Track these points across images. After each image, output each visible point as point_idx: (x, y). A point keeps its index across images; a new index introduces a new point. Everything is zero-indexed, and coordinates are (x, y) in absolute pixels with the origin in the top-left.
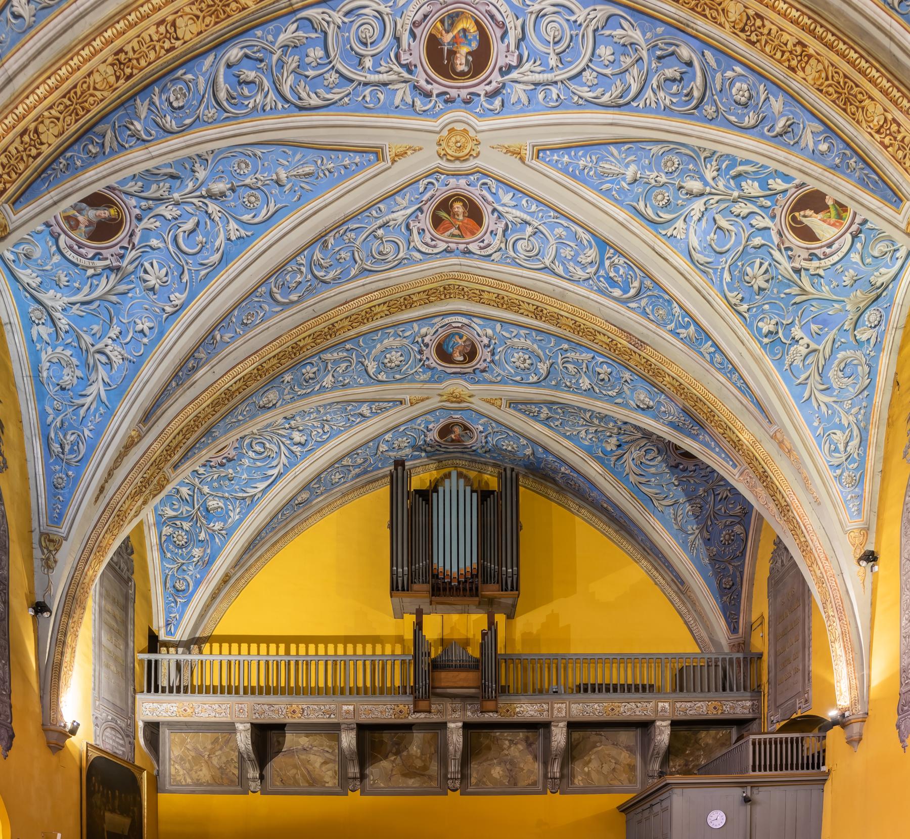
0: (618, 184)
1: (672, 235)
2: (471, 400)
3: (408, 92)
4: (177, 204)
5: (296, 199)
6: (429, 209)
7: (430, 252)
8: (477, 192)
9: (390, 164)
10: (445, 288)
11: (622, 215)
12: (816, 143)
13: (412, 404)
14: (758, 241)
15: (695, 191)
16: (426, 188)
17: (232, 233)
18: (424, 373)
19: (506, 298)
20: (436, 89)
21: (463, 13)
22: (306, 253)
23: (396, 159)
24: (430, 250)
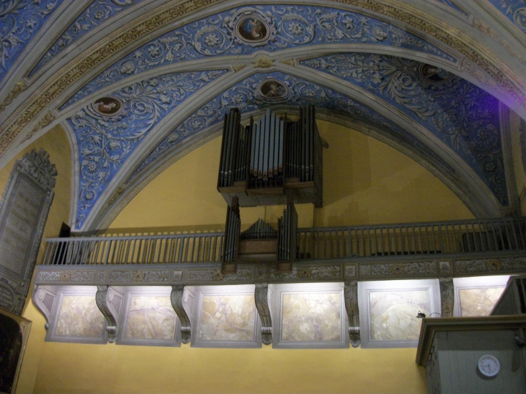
2: (274, 63)
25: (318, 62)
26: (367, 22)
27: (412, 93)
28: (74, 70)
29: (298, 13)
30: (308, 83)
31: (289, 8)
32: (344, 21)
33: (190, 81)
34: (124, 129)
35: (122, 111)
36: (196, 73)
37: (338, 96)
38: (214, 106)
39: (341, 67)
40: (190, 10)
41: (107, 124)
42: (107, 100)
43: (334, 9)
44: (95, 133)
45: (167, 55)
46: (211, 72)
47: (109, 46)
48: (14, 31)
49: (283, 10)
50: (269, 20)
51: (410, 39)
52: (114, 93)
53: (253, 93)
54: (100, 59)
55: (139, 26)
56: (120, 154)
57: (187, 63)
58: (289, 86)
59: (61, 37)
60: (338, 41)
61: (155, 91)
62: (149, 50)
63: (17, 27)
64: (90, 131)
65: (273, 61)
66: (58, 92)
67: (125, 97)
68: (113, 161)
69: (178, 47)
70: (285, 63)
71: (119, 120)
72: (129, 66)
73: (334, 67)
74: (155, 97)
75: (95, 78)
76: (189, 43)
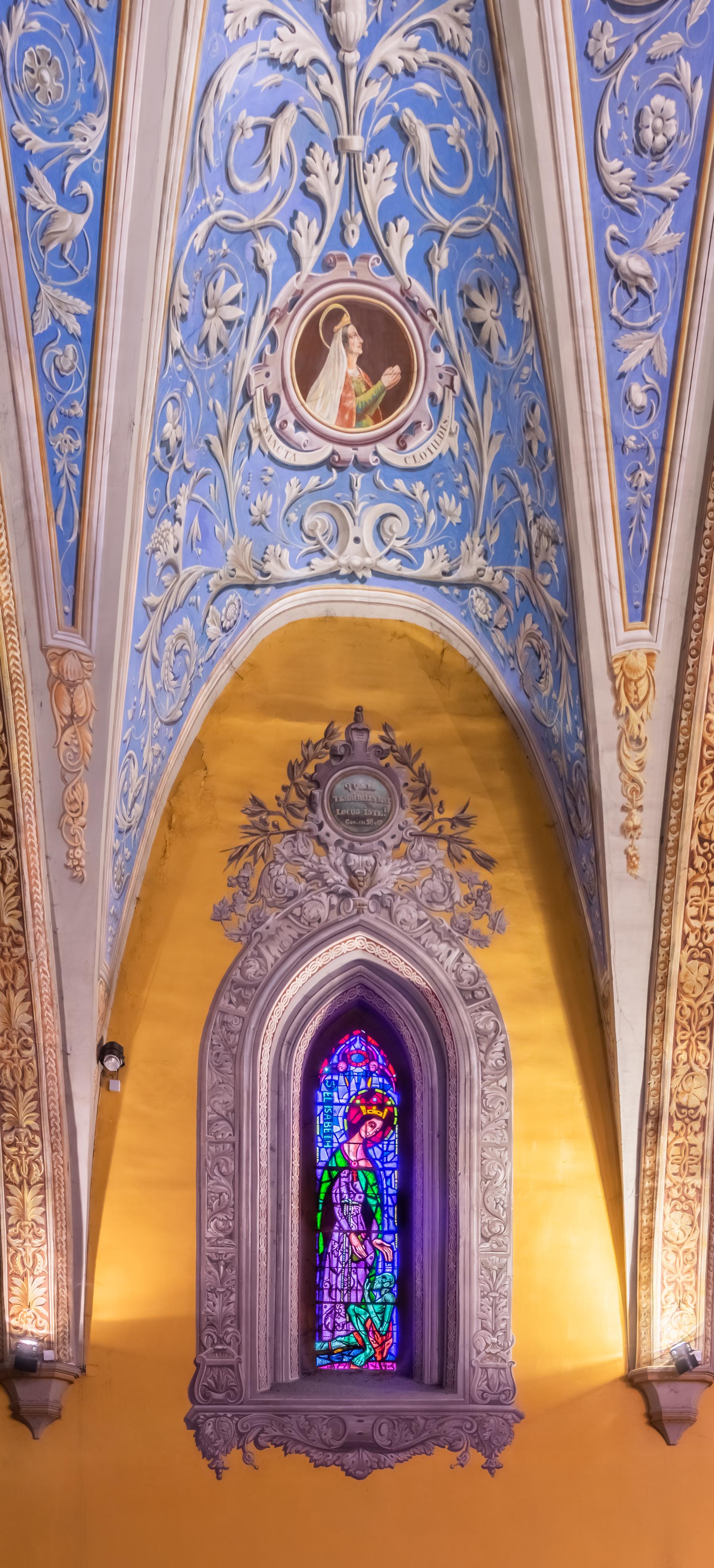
12: (637, 374)
15: (341, 16)
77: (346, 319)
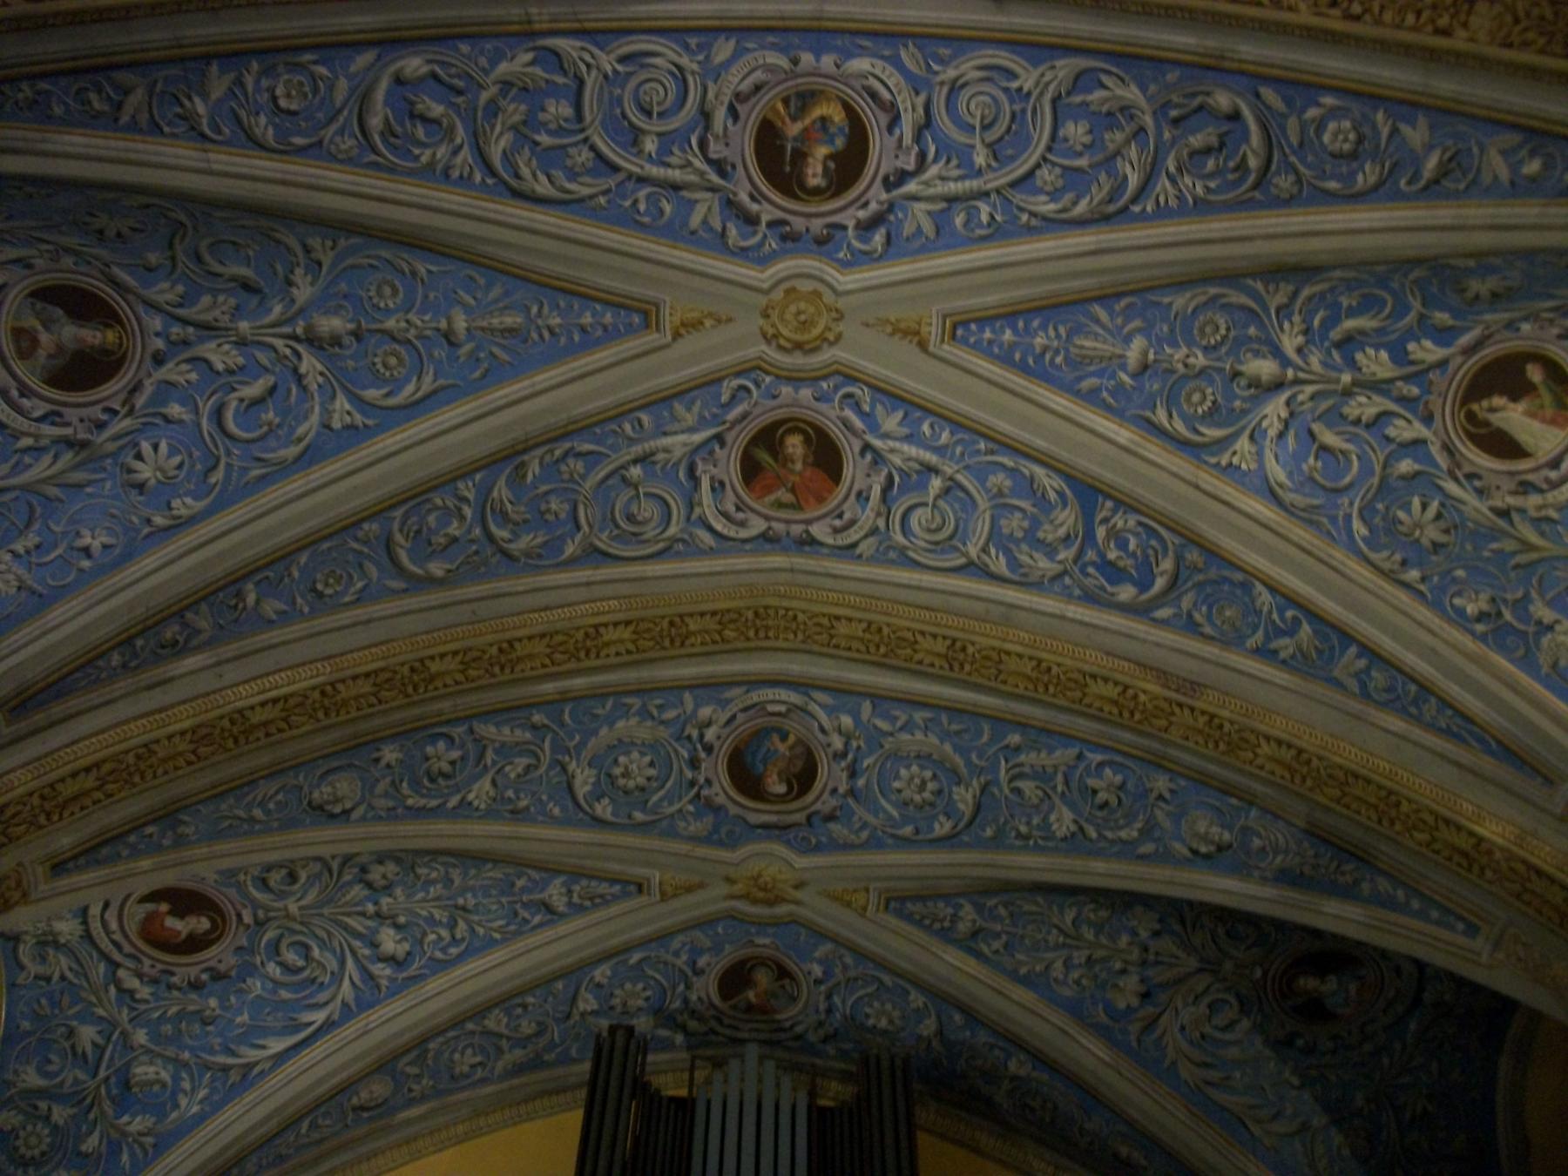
0: (1113, 376)
1: (1230, 464)
2: (799, 895)
3: (716, 208)
4: (242, 343)
5: (477, 374)
6: (738, 440)
7: (732, 534)
8: (833, 414)
9: (669, 338)
10: (756, 614)
11: (1124, 435)
12: (1514, 168)
13: (664, 897)
14: (1406, 466)
15: (1264, 378)
16: (733, 397)
17: (336, 416)
18: (698, 816)
19: (886, 630)
20: (767, 214)
21: (822, 92)
22: (478, 477)
23: (682, 331)
24: (731, 531)
25: (950, 910)
26: (1172, 791)
27: (1233, 1052)
28: (177, 739)
29: (945, 735)
30: (887, 979)
31: (919, 716)
32: (1091, 782)
33: (504, 900)
34: (205, 1023)
35: (221, 955)
36: (535, 875)
37: (983, 1037)
38: (548, 1007)
39: (1022, 937)
40: (613, 650)
41: (144, 992)
42: (185, 901)
43: (1068, 738)
44: (86, 1017)
45: (476, 786)
46: (584, 882)
47: (323, 693)
48: (22, 551)
49: (896, 718)
50: (838, 743)
51: (1316, 856)
52: (230, 875)
53: (688, 987)
54: (273, 730)
55: (442, 656)
56: (160, 1112)
57: (525, 830)
58: (818, 982)
59: (180, 614)
60: (1050, 844)
61: (370, 908)
62: (429, 750)
63: (37, 540)
64: (73, 1004)
65: (799, 886)
66: (87, 801)
67: (255, 905)
68: (125, 1134)
69: (520, 770)
70: (835, 898)
71: (196, 986)
72: (345, 787)
73: (998, 936)
74: (360, 929)
75: (222, 794)
76: (559, 762)
77: (1475, 407)
